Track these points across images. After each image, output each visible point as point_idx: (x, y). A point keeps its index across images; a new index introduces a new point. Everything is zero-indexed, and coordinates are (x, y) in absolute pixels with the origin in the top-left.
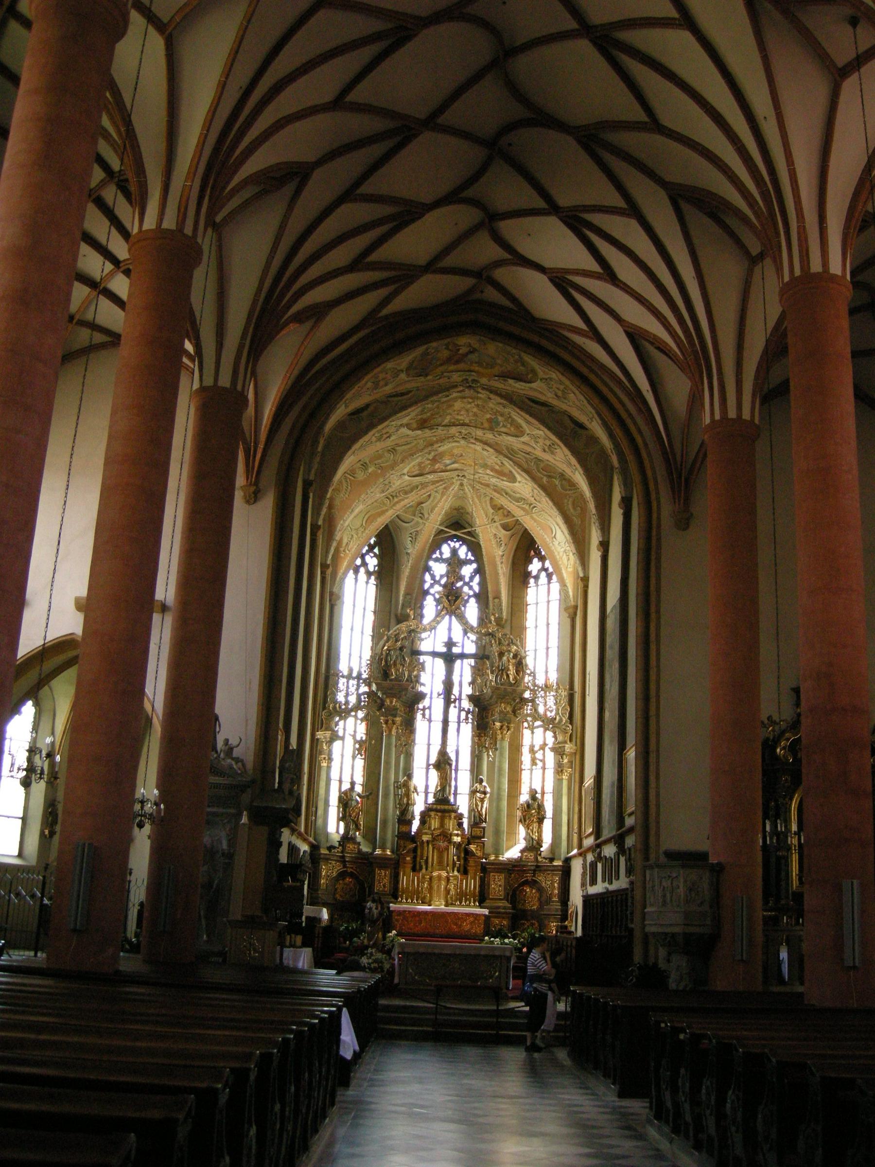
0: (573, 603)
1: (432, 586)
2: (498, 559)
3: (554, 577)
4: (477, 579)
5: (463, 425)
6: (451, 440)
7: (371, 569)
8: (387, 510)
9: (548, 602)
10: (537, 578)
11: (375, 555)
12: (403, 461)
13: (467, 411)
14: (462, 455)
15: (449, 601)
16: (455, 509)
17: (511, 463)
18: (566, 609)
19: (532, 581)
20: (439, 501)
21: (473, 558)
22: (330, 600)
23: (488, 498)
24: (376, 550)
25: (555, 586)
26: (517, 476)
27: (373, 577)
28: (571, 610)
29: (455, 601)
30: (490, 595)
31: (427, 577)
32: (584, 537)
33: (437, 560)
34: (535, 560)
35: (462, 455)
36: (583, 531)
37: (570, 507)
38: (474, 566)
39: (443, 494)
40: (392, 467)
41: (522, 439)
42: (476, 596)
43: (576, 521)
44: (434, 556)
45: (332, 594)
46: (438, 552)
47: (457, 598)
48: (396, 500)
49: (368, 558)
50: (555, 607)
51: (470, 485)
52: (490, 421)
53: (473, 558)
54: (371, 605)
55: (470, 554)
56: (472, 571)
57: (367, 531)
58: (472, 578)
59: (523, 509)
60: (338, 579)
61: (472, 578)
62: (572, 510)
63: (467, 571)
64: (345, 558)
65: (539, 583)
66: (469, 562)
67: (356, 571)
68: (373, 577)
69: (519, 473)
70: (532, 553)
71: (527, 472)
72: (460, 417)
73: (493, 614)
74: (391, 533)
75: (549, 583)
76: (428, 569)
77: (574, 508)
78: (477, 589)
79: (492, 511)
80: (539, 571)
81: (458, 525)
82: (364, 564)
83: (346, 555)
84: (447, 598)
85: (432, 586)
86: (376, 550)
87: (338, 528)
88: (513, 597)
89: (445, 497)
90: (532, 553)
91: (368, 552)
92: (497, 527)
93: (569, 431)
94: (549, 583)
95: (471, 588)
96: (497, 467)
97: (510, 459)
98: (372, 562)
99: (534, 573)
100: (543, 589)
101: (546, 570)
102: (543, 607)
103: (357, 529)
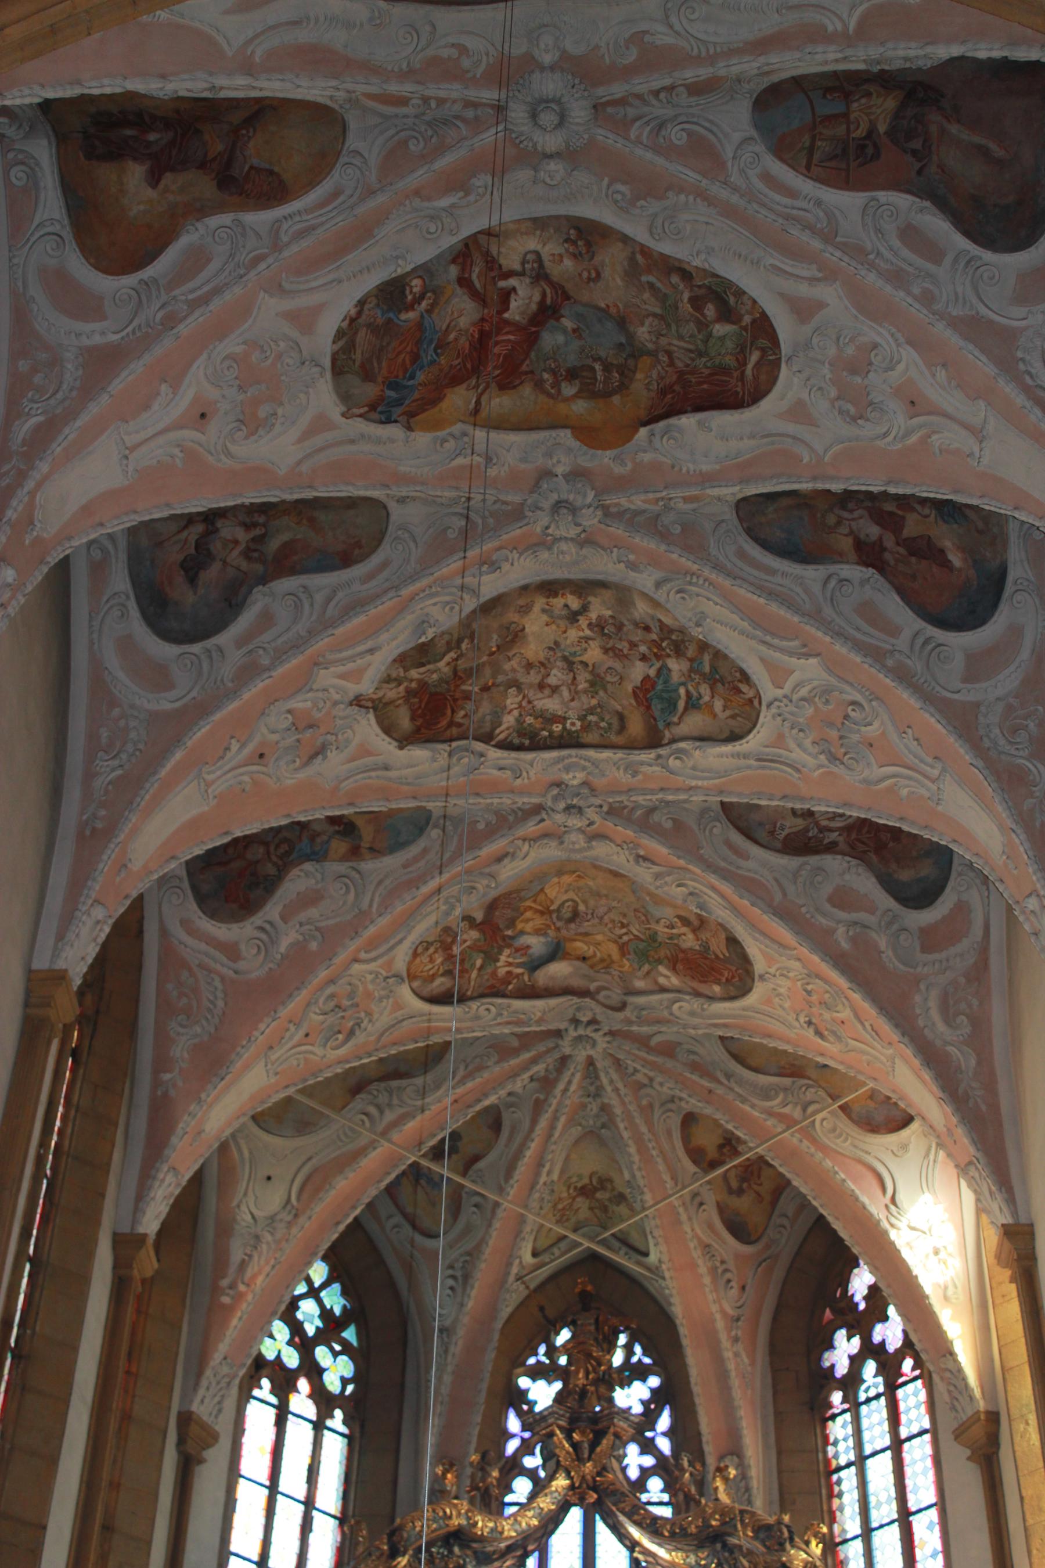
0: (982, 1405)
1: (526, 1448)
2: (720, 1324)
3: (908, 1364)
4: (664, 1422)
5: (568, 741)
6: (531, 828)
7: (332, 1382)
8: (362, 1152)
9: (897, 1445)
10: (851, 1382)
11: (347, 1349)
12: (385, 906)
13: (570, 664)
14: (575, 915)
15: (575, 1446)
16: (585, 1191)
17: (726, 888)
18: (958, 1435)
19: (837, 1397)
20: (528, 1138)
21: (647, 1360)
22: (181, 1441)
23: (675, 1122)
24: (350, 1334)
25: (913, 1398)
26: (753, 949)
27: (338, 1414)
28: (978, 1431)
29: (594, 1445)
30: (708, 1449)
31: (513, 1424)
32: (995, 1107)
33: (537, 1373)
34: (841, 1335)
35: (575, 915)
36: (990, 1087)
37: (935, 1015)
38: (654, 1381)
39: (538, 1107)
40: (353, 928)
41: (752, 743)
42: (663, 1467)
43: (965, 1060)
44: (532, 1361)
45: (186, 1419)
46: (542, 1349)
47: (599, 1435)
48: (389, 1116)
49: (322, 1354)
50: (919, 1455)
51: (617, 1063)
52: (644, 692)
53: (647, 1360)
54: (330, 1495)
55: (638, 1349)
56: (646, 1395)
57: (301, 1220)
58: (649, 1417)
59: (781, 1117)
60: (208, 1373)
61: (649, 1417)
62: (941, 1027)
63: (631, 1397)
64: (230, 1310)
65: (862, 1397)
66: (640, 1373)
67: (284, 1382)
68: (338, 1414)
69: (753, 926)
70: (828, 1314)
71: (786, 914)
72: (551, 704)
73: (719, 1470)
74: (392, 1285)
75: (891, 1388)
76: (518, 1399)
77: (948, 1022)
78: (664, 1445)
79: (692, 1168)
80: (856, 1362)
81: (600, 1296)
82: (313, 1371)
83: (240, 1297)
84: (568, 1434)
85: (526, 1448)
86: (350, 1334)
87: (179, 1131)
88: (779, 1453)
89: (543, 1123)
90: (828, 1314)
91: (324, 1336)
92: (711, 1227)
93: (902, 642)
94: (891, 1388)
95: (648, 1447)
96: (689, 941)
97: (725, 875)
98: (337, 1370)
99: (842, 1368)
100: (874, 1417)
101: (872, 1350)
102: (880, 1470)
103: (272, 1218)
